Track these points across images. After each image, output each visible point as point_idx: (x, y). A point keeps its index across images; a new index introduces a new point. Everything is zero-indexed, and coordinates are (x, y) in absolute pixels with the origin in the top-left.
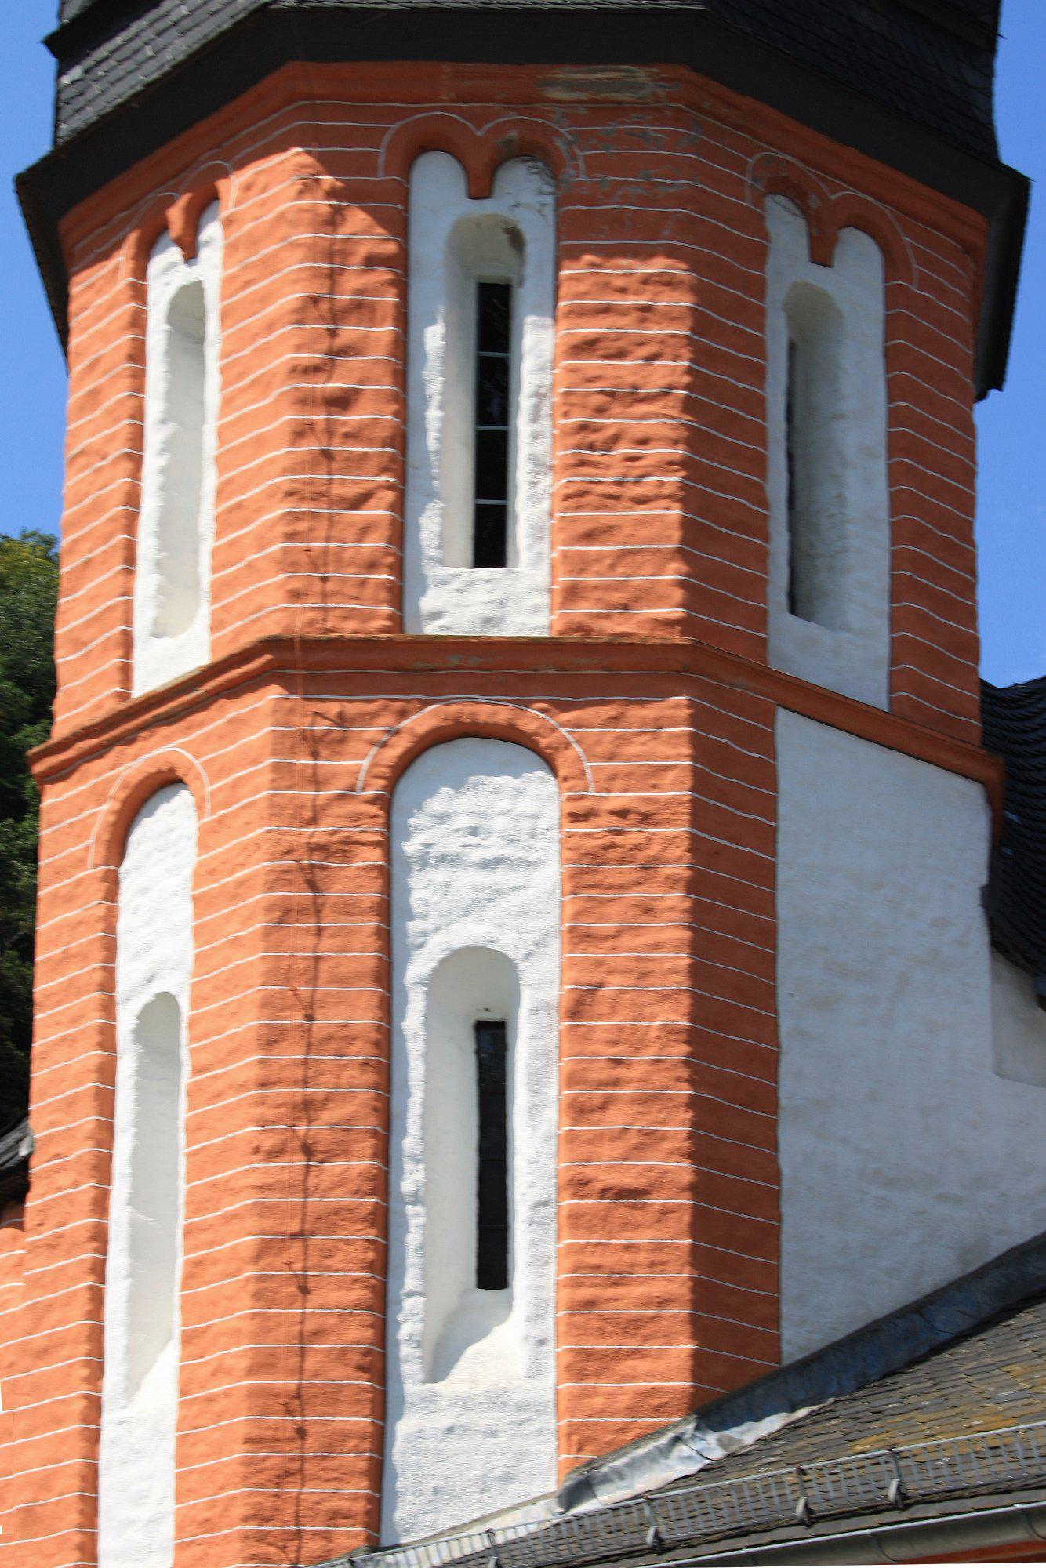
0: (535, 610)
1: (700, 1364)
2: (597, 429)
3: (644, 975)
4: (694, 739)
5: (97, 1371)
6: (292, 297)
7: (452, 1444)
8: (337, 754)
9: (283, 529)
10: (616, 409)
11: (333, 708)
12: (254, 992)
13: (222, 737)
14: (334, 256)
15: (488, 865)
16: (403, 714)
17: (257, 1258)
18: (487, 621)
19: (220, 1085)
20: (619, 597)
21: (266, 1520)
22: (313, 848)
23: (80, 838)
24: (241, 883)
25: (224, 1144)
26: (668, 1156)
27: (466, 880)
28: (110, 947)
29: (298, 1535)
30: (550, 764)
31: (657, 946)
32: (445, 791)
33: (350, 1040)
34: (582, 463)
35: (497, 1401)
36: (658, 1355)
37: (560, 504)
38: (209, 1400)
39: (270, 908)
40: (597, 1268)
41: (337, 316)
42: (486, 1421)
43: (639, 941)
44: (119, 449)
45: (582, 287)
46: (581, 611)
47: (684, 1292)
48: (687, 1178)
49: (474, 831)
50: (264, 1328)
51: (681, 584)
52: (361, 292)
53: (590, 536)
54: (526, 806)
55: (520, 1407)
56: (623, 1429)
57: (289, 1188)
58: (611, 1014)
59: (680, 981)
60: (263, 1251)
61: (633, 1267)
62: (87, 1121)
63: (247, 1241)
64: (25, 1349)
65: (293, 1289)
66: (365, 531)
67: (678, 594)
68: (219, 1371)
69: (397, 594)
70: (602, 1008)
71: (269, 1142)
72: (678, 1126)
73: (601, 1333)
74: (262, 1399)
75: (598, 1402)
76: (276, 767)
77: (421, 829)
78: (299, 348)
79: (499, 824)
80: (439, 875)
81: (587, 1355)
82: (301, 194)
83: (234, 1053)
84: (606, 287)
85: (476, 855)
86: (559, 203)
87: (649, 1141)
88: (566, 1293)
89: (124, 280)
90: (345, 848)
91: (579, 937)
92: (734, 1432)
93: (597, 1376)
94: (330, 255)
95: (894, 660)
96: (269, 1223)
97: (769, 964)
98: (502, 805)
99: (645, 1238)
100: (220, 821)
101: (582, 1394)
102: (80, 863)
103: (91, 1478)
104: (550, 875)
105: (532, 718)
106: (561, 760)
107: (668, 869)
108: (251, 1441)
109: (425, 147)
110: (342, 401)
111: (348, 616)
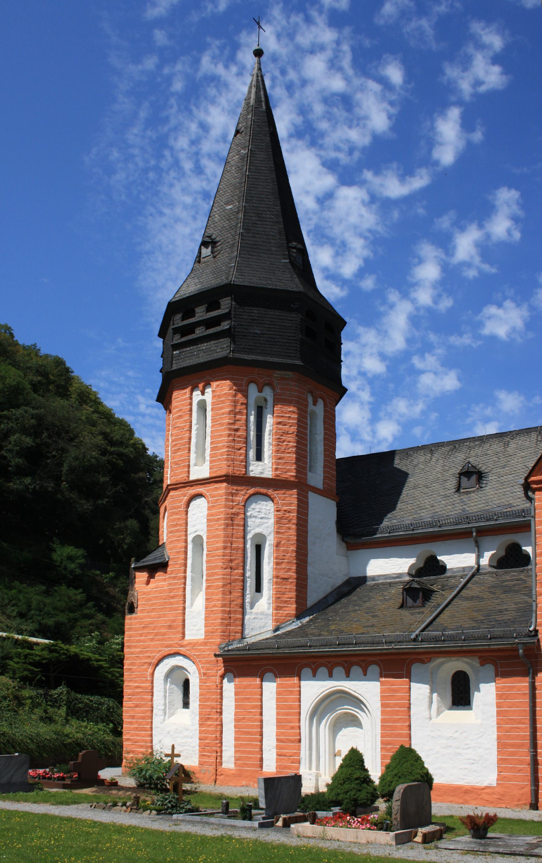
0: (269, 471)
1: (297, 609)
2: (281, 439)
3: (288, 540)
4: (298, 498)
5: (185, 602)
6: (228, 410)
7: (255, 621)
8: (236, 497)
9: (226, 453)
10: (284, 435)
11: (235, 488)
12: (222, 539)
14: (235, 402)
15: (262, 518)
16: (248, 490)
17: (222, 587)
18: (261, 473)
19: (214, 554)
20: (284, 470)
21: (224, 633)
22: (232, 514)
23: (179, 502)
24: (218, 518)
26: (292, 573)
27: (258, 521)
28: (186, 524)
29: (230, 635)
31: (291, 535)
32: (254, 504)
33: (239, 549)
34: (278, 445)
35: (262, 613)
36: (290, 607)
37: (274, 452)
38: (212, 611)
39: (225, 524)
40: (280, 592)
41: (236, 414)
42: (261, 617)
43: (288, 534)
44: (187, 428)
45: (279, 412)
46: (278, 472)
47: (295, 597)
48: (295, 577)
49: (259, 512)
50: (224, 599)
51: (295, 469)
52: (240, 409)
53: (280, 459)
54: (268, 508)
55: (266, 615)
56: (284, 619)
57: (227, 575)
58: (283, 547)
59: (294, 542)
60: (224, 586)
61: (286, 592)
62: (183, 556)
63: (221, 584)
65: (228, 593)
66: (240, 455)
67: (295, 471)
68: (214, 606)
69: (246, 467)
70: (281, 545)
71: (224, 567)
72: (294, 568)
73: (281, 603)
74: (224, 612)
75: (280, 615)
76: (226, 498)
77: (250, 511)
78: (229, 419)
79: (263, 511)
80: (253, 519)
81: (278, 606)
82: (230, 390)
83: (217, 549)
84: (283, 412)
85: (260, 516)
86: (274, 396)
87: (289, 570)
88: (274, 596)
89: (188, 396)
90: (238, 514)
91: (277, 533)
92: (301, 620)
93: (280, 610)
94: (235, 402)
95: (324, 480)
96: (225, 581)
97: (307, 537)
98: (264, 507)
99: (288, 587)
100: (213, 506)
101: (277, 613)
102: (180, 507)
103: (184, 621)
104: (272, 521)
105: (270, 492)
106: (275, 500)
107: (293, 521)
108: (222, 619)
109: (251, 382)
110: (237, 430)
111: (238, 470)
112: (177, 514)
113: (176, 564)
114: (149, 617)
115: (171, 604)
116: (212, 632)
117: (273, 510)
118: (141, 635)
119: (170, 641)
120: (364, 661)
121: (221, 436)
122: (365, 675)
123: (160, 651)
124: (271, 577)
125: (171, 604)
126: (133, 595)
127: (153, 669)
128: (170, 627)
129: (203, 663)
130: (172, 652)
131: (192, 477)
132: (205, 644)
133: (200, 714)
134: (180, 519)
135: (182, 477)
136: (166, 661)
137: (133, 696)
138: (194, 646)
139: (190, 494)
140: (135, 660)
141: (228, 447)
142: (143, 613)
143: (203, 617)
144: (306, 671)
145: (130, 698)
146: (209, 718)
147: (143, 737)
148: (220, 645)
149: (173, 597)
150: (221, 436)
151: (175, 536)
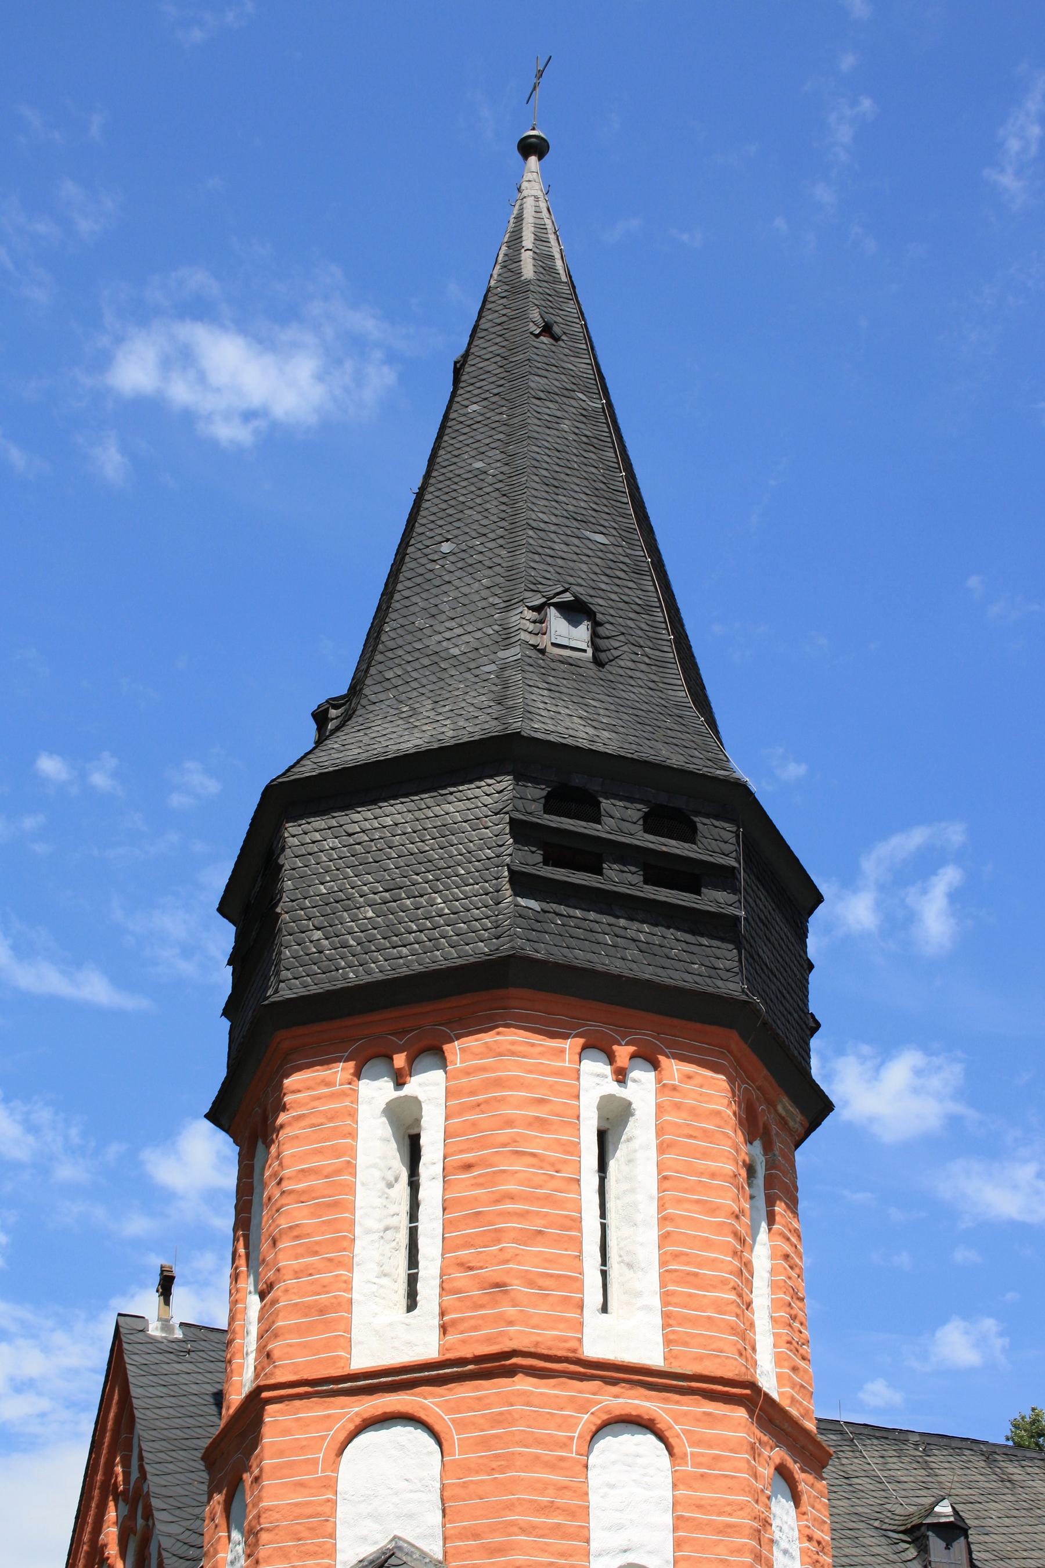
2: (792, 1308)
13: (698, 1420)
16: (772, 1449)
30: (797, 1504)
100: (702, 1475)
112: (551, 1466)
117: (796, 1534)
121: (708, 1244)
131: (593, 1349)
134: (565, 1488)
135: (565, 1340)
141: (734, 1288)
150: (708, 1244)
151: (544, 1550)
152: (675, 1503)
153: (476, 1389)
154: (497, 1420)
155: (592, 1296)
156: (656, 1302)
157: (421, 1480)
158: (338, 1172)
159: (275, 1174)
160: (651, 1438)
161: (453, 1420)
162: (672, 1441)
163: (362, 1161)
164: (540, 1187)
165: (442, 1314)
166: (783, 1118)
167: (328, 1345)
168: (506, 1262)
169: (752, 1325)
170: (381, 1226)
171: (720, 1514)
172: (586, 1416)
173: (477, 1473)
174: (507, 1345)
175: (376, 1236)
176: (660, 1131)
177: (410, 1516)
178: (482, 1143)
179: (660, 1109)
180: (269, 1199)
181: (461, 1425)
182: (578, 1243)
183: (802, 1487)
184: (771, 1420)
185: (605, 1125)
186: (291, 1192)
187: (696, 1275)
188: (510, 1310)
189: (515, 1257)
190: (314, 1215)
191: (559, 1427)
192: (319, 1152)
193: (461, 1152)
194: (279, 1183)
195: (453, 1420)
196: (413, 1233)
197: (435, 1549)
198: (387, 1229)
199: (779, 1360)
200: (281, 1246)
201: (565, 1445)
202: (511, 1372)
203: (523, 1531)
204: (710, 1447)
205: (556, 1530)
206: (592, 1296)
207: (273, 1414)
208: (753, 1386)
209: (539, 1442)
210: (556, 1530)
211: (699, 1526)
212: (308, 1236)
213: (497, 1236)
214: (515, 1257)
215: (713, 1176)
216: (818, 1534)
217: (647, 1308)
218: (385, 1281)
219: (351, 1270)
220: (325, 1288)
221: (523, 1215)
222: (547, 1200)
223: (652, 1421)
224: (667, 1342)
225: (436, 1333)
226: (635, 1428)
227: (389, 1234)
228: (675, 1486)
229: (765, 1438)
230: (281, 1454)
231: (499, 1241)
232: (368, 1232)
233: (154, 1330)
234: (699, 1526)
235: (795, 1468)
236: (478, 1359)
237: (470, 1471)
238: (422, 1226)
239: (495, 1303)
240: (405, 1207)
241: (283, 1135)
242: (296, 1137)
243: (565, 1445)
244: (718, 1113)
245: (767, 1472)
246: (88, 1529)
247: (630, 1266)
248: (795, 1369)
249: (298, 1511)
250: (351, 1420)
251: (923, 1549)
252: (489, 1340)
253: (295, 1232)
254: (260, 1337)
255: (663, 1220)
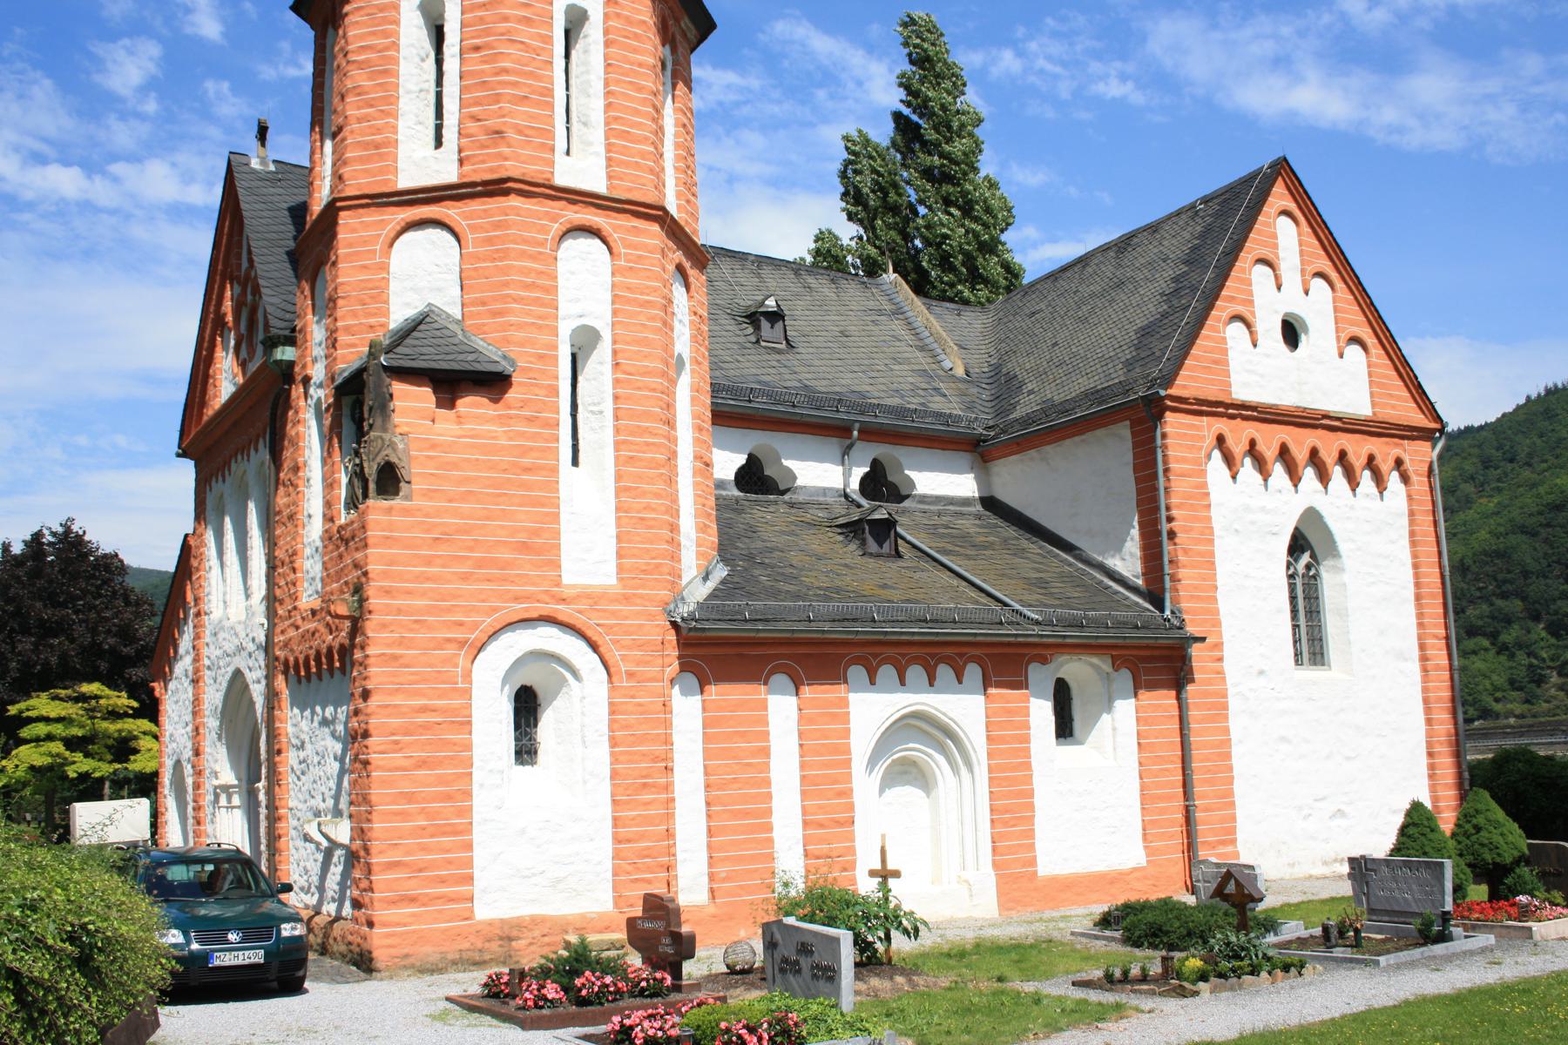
19: (640, 384)
24: (648, 302)
25: (644, 411)
64: (514, 464)
68: (648, 508)
100: (631, 268)
113: (536, 385)
114: (456, 513)
115: (524, 485)
116: (644, 572)
118: (429, 561)
119: (526, 584)
120: (961, 655)
121: (637, 112)
122: (872, 682)
123: (495, 610)
124: (691, 458)
125: (524, 485)
126: (392, 445)
127: (472, 657)
128: (524, 547)
129: (623, 647)
130: (535, 615)
131: (561, 180)
132: (627, 599)
133: (614, 775)
135: (542, 172)
136: (507, 638)
137: (406, 734)
138: (596, 604)
139: (569, 221)
140: (411, 630)
142: (431, 499)
143: (613, 531)
144: (857, 673)
145: (396, 742)
146: (645, 785)
147: (448, 851)
148: (667, 604)
149: (527, 470)
150: (637, 112)
152: (614, 286)
153: (484, 204)
154: (498, 226)
155: (560, 144)
156: (602, 150)
157: (446, 265)
158: (387, 49)
159: (342, 49)
160: (597, 242)
161: (468, 225)
162: (612, 244)
163: (403, 41)
164: (527, 65)
165: (460, 151)
166: (683, 31)
167: (382, 171)
168: (504, 116)
169: (663, 169)
170: (417, 88)
171: (642, 294)
172: (556, 225)
173: (484, 261)
174: (504, 174)
175: (414, 96)
176: (606, 32)
177: (439, 290)
178: (487, 32)
179: (606, 17)
180: (339, 67)
181: (473, 228)
182: (551, 106)
183: (691, 279)
184: (674, 234)
185: (570, 26)
186: (354, 62)
187: (628, 132)
188: (506, 150)
189: (510, 114)
190: (370, 79)
191: (539, 232)
192: (373, 33)
193: (473, 38)
194: (345, 55)
195: (468, 225)
196: (439, 97)
197: (456, 312)
198: (421, 91)
199: (679, 195)
200: (348, 100)
201: (542, 244)
202: (506, 193)
203: (516, 300)
204: (636, 249)
205: (537, 302)
206: (560, 143)
207: (345, 219)
208: (663, 209)
209: (525, 241)
210: (537, 302)
211: (628, 301)
212: (367, 93)
213: (497, 99)
214: (510, 114)
215: (640, 65)
216: (700, 311)
217: (597, 154)
218: (419, 127)
219: (397, 119)
220: (379, 131)
221: (515, 85)
222: (531, 75)
223: (599, 230)
224: (610, 177)
225: (456, 164)
226: (585, 234)
227: (423, 95)
228: (613, 274)
229: (671, 244)
230: (350, 245)
231: (498, 102)
232: (409, 92)
233: (255, 164)
234: (628, 301)
235: (687, 265)
236: (485, 183)
237: (479, 259)
238: (446, 90)
239: (496, 145)
240: (433, 76)
241: (347, 21)
242: (357, 22)
243: (542, 244)
244: (644, 22)
245: (671, 268)
246: (214, 303)
247: (585, 124)
248: (688, 201)
249: (363, 285)
250: (398, 223)
251: (757, 328)
252: (491, 170)
253: (358, 90)
254: (334, 164)
255: (608, 94)
